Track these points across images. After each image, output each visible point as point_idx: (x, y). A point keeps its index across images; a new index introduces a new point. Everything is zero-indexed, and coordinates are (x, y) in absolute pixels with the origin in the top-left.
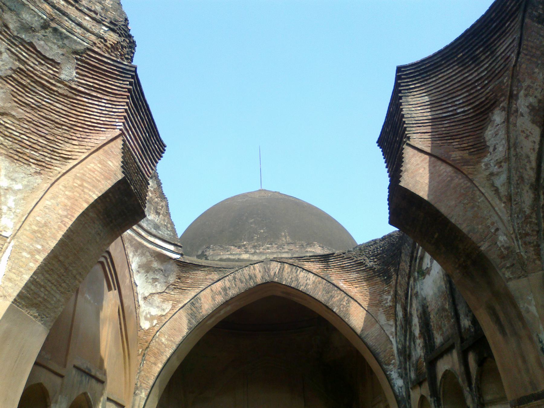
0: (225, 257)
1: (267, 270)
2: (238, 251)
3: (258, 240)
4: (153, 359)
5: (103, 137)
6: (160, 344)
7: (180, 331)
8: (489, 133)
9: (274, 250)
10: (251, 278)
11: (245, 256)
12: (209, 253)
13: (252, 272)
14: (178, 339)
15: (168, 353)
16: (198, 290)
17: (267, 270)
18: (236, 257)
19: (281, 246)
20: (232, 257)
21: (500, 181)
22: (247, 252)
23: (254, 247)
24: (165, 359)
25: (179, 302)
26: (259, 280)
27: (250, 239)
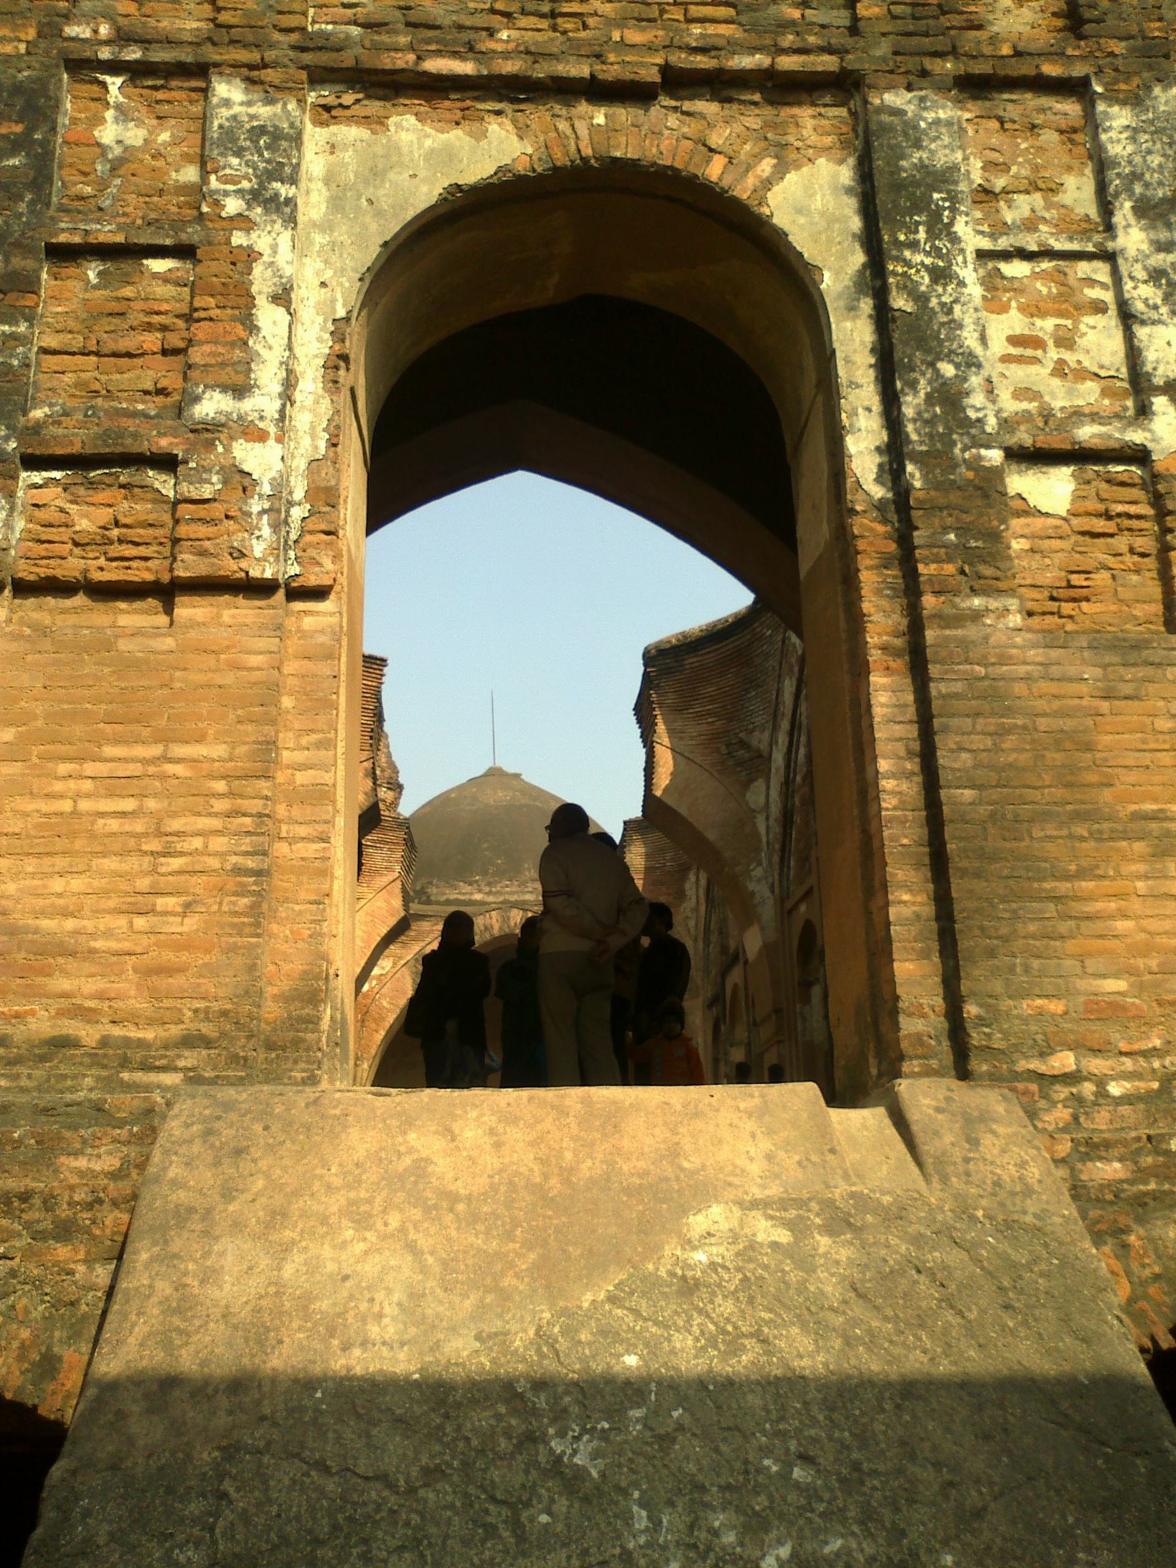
0: (452, 897)
1: (505, 920)
2: (468, 889)
3: (494, 875)
4: (373, 1026)
5: (385, 880)
6: (382, 1008)
7: (405, 993)
8: (687, 886)
9: (514, 889)
10: (486, 928)
11: (478, 897)
12: (433, 890)
13: (488, 922)
14: (403, 1001)
15: (391, 1018)
16: (422, 944)
17: (505, 920)
18: (467, 897)
19: (523, 884)
20: (461, 897)
21: (692, 923)
22: (480, 891)
23: (489, 884)
24: (387, 1025)
25: (400, 958)
26: (496, 932)
27: (485, 873)
